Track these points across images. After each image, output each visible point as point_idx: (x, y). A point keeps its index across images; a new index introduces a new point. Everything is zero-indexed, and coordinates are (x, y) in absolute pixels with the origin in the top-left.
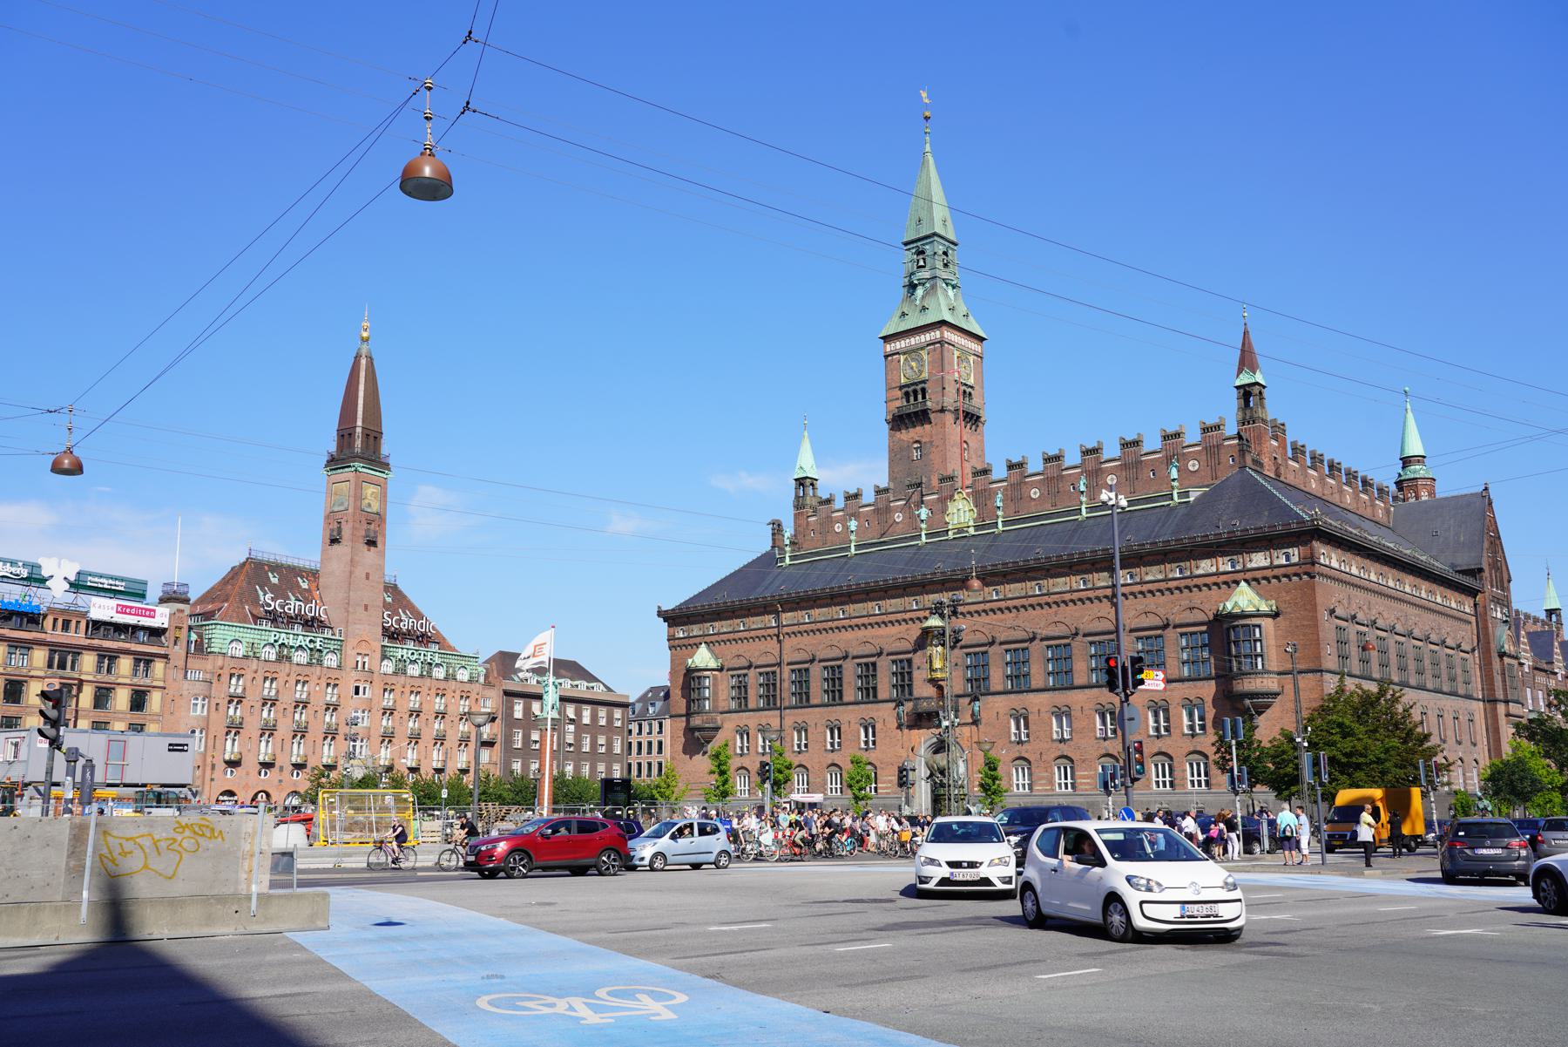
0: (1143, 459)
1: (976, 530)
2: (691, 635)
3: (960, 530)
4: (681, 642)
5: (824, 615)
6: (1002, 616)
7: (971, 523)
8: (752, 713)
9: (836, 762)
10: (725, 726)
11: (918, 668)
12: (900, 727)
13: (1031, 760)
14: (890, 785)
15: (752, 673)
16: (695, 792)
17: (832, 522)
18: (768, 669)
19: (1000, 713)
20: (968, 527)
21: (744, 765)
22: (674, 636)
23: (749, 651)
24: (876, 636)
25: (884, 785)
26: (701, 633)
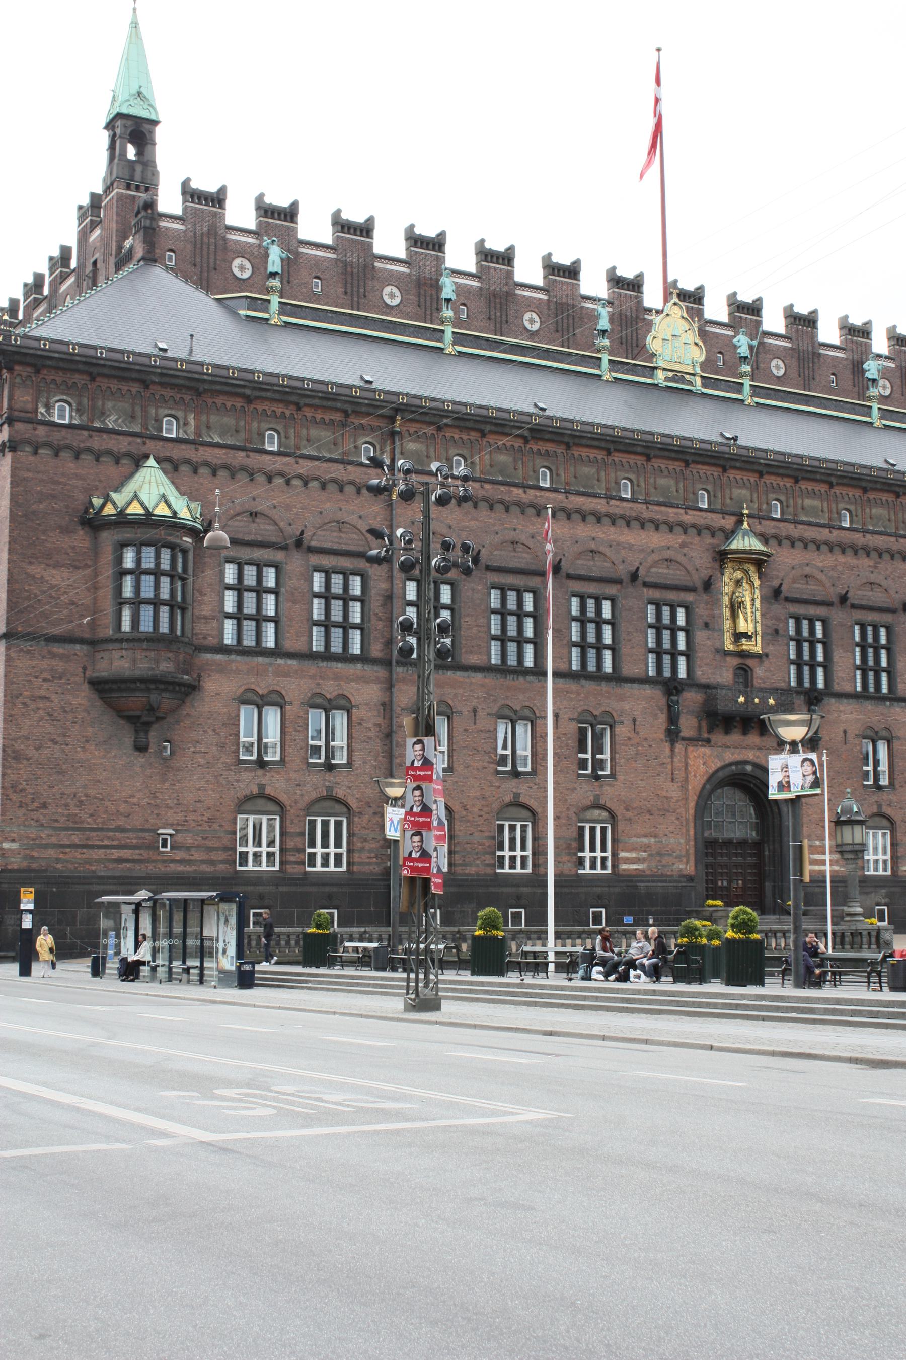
0: (821, 351)
1: (704, 385)
2: (97, 424)
3: (678, 376)
4: (57, 437)
5: (501, 472)
6: (854, 561)
7: (698, 370)
8: (290, 662)
9: (522, 799)
10: (211, 685)
11: (706, 625)
12: (673, 735)
13: (895, 819)
14: (644, 855)
15: (295, 563)
16: (101, 853)
17: (225, 249)
18: (346, 563)
19: (849, 732)
20: (694, 375)
21: (269, 791)
22: (36, 411)
23: (288, 508)
24: (618, 544)
25: (634, 855)
26: (137, 429)
